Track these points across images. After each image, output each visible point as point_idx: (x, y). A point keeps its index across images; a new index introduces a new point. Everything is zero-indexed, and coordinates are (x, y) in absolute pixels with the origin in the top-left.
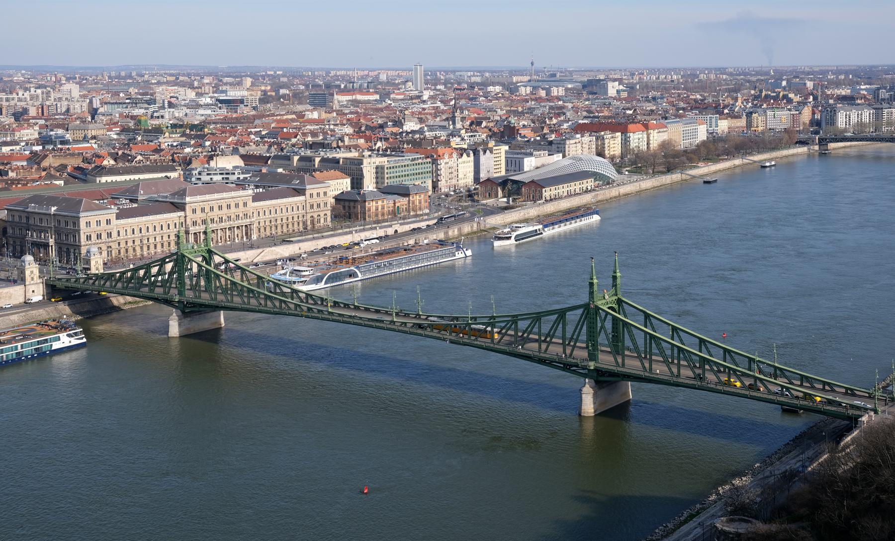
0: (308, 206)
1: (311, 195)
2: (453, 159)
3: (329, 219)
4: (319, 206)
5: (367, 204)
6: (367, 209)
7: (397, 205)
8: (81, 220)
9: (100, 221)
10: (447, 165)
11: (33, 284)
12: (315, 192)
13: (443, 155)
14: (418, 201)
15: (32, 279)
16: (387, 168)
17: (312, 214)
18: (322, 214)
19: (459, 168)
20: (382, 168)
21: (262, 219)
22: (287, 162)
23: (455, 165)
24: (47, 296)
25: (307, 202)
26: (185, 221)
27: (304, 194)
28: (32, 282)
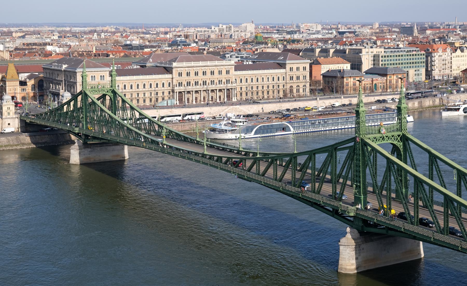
0: (288, 78)
1: (291, 69)
2: (447, 53)
3: (308, 90)
4: (298, 78)
5: (345, 79)
6: (345, 83)
7: (374, 82)
8: (77, 74)
9: (95, 76)
10: (440, 58)
12: (295, 67)
13: (438, 49)
15: (9, 114)
16: (382, 57)
17: (291, 85)
18: (301, 85)
19: (452, 61)
20: (378, 56)
22: (312, 54)
23: (449, 58)
24: (21, 129)
27: (285, 68)
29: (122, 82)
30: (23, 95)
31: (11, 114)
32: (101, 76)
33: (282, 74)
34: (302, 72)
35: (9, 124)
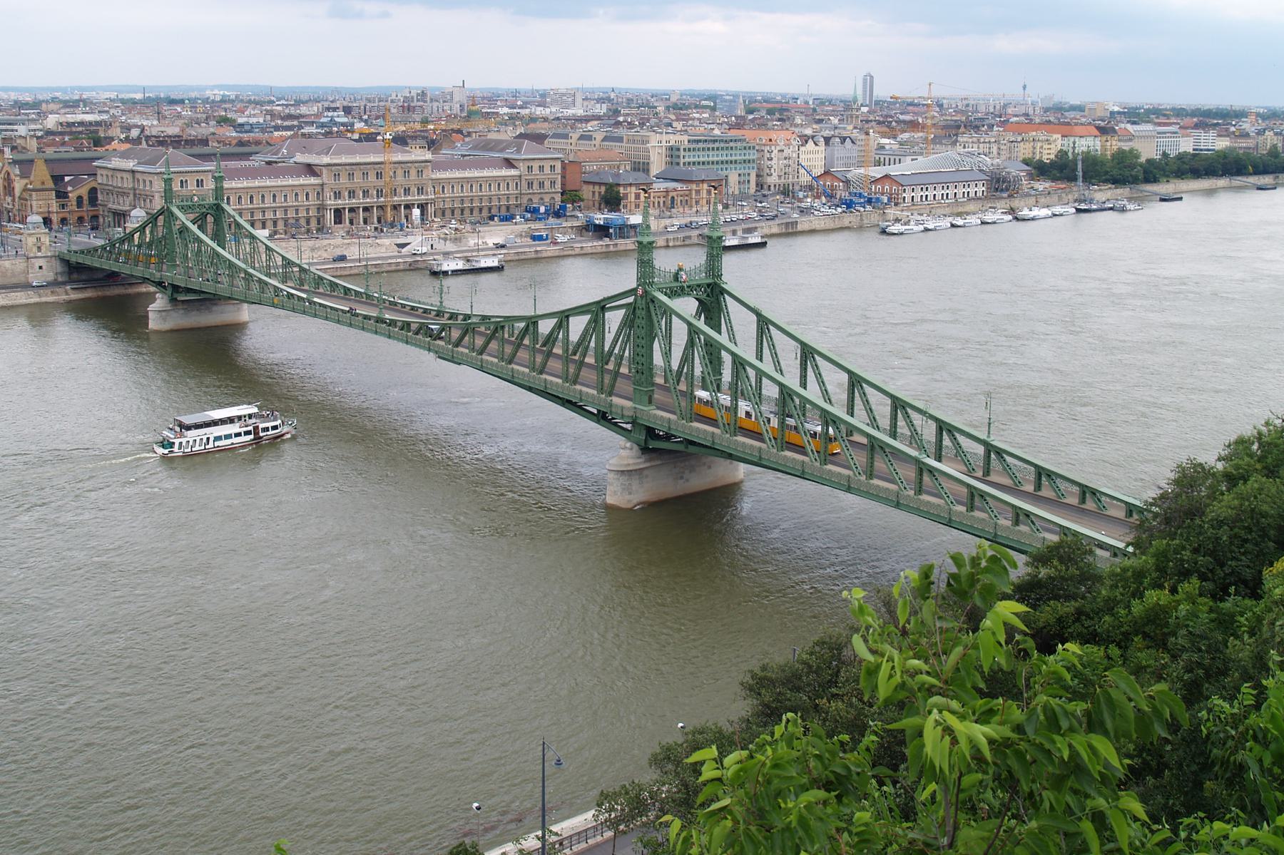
4: (541, 185)
9: (186, 181)
10: (780, 153)
11: (41, 257)
14: (705, 191)
15: (39, 248)
21: (449, 197)
25: (523, 178)
26: (323, 189)
28: (39, 254)
29: (234, 191)
30: (61, 215)
31: (43, 249)
32: (198, 180)
34: (549, 174)
35: (41, 268)
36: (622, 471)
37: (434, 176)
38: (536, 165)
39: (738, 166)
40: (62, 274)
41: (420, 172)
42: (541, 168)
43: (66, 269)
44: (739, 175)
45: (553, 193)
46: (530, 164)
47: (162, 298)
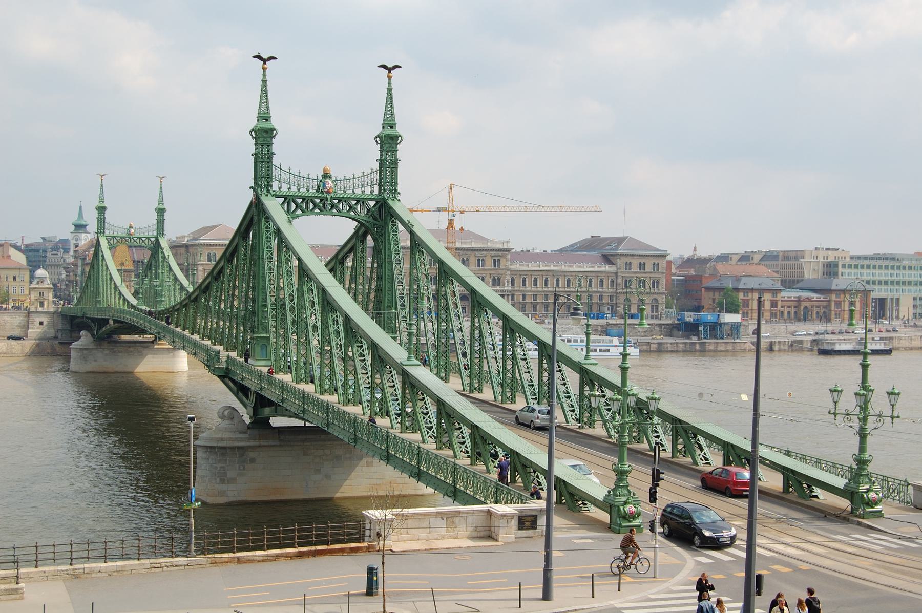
21: (530, 291)
25: (620, 275)
33: (609, 275)
34: (651, 273)
36: (211, 447)
37: (513, 268)
38: (635, 263)
39: (913, 288)
40: (63, 330)
41: (496, 263)
42: (642, 266)
43: (68, 327)
44: (915, 299)
45: (656, 293)
46: (628, 260)
47: (86, 336)
